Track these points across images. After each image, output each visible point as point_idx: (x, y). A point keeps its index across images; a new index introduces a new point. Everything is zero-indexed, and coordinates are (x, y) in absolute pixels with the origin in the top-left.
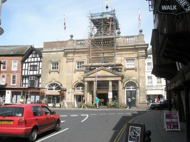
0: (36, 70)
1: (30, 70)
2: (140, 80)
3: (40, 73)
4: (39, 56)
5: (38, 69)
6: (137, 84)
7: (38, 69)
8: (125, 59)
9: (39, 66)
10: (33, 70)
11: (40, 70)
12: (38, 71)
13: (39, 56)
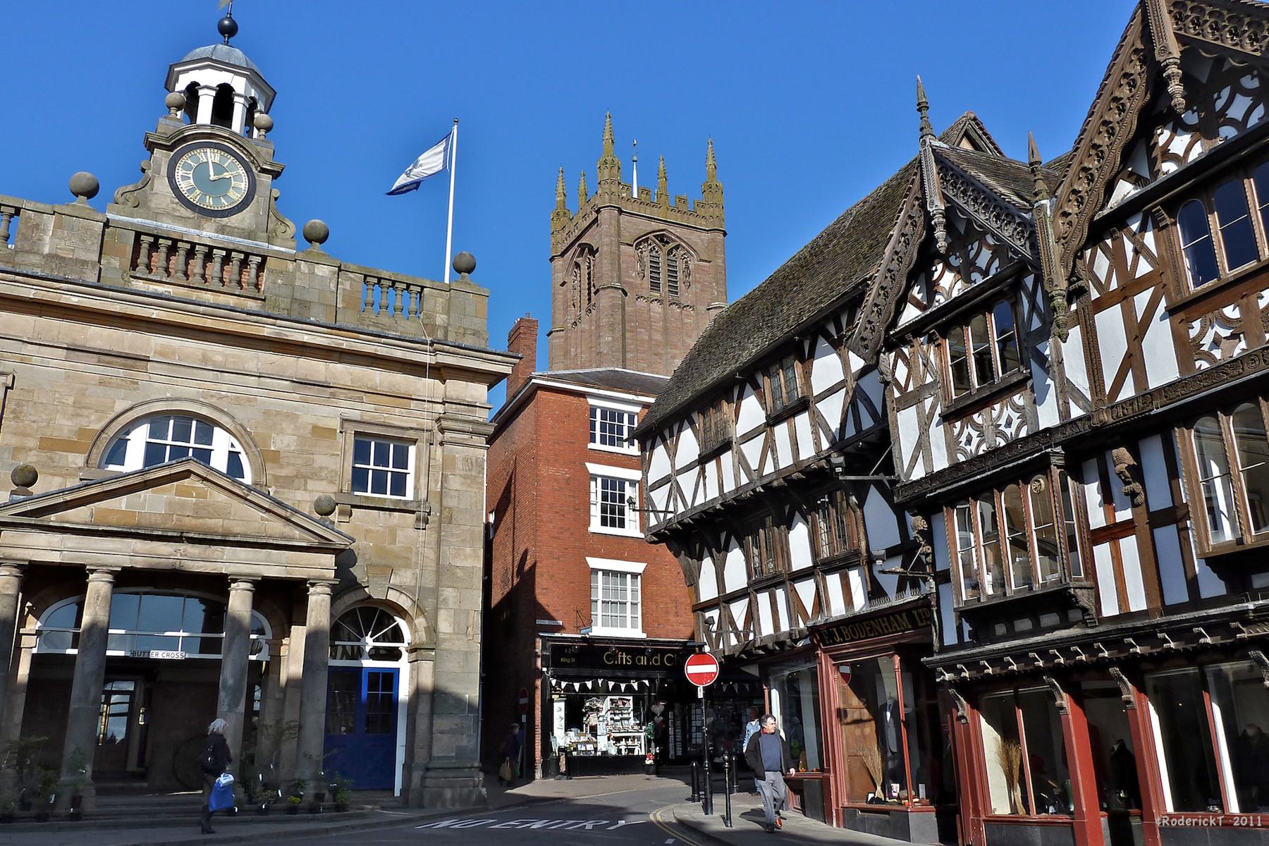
2: (448, 593)
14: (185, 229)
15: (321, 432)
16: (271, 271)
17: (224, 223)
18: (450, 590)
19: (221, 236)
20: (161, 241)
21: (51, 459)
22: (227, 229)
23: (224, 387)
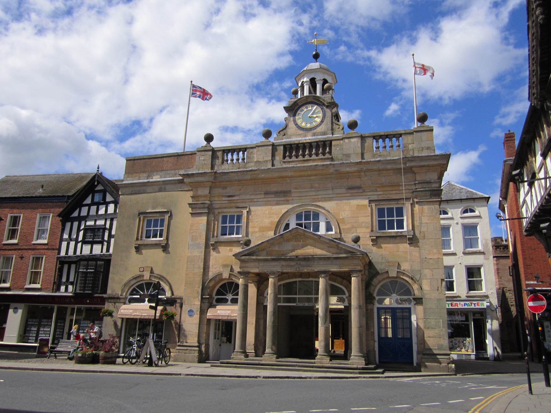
0: (102, 243)
1: (84, 242)
2: (427, 272)
3: (111, 251)
4: (112, 199)
5: (106, 238)
6: (415, 287)
7: (106, 238)
10: (92, 243)
11: (112, 240)
12: (105, 243)
13: (112, 199)
14: (300, 139)
16: (334, 145)
17: (315, 132)
18: (427, 270)
19: (314, 137)
20: (293, 146)
21: (263, 234)
22: (316, 134)
23: (320, 197)
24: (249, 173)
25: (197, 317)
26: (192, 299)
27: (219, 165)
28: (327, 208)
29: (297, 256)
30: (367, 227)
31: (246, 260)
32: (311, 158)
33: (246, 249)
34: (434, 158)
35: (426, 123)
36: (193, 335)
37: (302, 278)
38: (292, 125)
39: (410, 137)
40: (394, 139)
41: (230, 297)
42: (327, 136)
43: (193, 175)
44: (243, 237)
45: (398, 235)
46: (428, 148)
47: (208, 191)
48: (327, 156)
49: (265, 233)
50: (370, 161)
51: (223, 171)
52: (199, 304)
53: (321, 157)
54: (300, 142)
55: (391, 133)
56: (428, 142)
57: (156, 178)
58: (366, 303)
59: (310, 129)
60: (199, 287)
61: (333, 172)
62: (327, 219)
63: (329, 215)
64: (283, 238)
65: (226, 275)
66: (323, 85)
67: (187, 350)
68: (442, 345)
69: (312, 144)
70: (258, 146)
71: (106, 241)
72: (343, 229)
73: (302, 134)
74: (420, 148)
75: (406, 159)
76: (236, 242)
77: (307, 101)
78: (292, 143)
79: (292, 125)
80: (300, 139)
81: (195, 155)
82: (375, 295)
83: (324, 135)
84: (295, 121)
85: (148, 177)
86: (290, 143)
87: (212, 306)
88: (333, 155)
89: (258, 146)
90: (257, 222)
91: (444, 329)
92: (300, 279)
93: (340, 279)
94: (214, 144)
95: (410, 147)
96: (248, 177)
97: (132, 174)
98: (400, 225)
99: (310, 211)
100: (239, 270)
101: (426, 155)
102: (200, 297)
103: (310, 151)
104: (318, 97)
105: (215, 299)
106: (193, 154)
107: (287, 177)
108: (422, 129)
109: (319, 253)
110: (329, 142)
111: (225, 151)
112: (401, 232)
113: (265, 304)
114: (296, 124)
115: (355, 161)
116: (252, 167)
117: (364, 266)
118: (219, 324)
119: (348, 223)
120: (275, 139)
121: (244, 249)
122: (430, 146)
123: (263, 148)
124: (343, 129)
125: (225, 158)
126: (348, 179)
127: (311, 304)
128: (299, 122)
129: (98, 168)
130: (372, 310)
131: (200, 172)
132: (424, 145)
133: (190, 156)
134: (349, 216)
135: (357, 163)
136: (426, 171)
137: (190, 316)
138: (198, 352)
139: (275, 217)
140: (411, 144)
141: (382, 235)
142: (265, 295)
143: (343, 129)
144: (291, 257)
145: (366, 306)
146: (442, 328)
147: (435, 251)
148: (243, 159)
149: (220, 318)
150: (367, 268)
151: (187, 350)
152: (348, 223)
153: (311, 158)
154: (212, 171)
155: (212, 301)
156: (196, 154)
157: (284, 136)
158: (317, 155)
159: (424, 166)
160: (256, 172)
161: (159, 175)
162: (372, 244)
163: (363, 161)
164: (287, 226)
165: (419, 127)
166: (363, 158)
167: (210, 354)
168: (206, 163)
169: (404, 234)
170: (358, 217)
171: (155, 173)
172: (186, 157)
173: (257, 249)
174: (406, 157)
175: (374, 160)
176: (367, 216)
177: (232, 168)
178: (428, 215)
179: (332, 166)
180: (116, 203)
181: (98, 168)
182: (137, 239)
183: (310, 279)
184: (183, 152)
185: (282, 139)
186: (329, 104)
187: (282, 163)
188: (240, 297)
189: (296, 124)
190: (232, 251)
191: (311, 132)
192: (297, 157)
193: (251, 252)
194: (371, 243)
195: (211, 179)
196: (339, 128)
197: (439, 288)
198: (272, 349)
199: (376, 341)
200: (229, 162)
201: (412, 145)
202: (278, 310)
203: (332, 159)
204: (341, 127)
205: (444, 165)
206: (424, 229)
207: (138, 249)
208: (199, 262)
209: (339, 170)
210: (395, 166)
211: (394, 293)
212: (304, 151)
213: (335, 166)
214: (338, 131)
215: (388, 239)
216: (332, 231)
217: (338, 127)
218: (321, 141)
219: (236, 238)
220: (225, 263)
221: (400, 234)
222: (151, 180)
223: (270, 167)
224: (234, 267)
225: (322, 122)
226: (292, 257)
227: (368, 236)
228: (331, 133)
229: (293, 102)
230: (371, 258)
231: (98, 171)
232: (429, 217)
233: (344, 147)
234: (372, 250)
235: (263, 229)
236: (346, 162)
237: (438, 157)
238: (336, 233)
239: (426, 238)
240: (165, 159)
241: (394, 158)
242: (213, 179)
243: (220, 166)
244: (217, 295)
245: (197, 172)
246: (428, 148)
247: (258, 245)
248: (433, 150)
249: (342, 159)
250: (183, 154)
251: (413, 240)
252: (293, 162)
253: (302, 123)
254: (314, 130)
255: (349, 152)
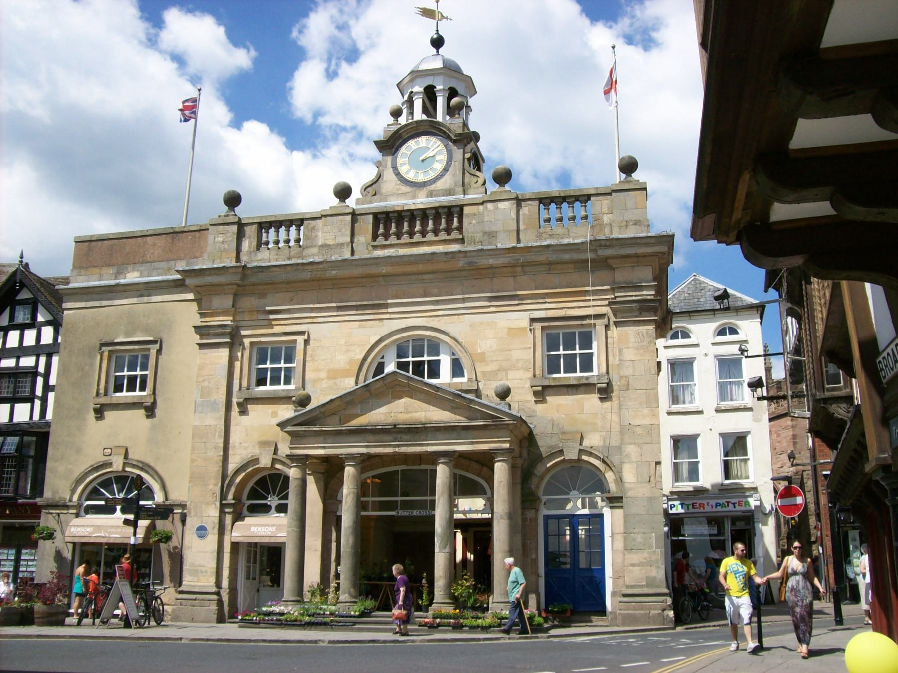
0: (31, 400)
3: (49, 416)
5: (39, 392)
6: (610, 476)
7: (39, 392)
8: (538, 326)
9: (47, 376)
11: (51, 396)
12: (38, 403)
14: (405, 202)
15: (513, 332)
16: (468, 215)
17: (432, 189)
18: (632, 446)
19: (430, 199)
21: (335, 384)
22: (434, 193)
24: (308, 267)
25: (212, 539)
26: (203, 506)
27: (251, 252)
28: (452, 334)
29: (395, 425)
30: (527, 370)
31: (301, 432)
32: (424, 239)
33: (300, 412)
34: (644, 241)
35: (635, 176)
36: (206, 572)
37: (407, 465)
38: (389, 175)
39: (605, 202)
40: (577, 204)
41: (273, 501)
42: (455, 197)
43: (201, 270)
44: (297, 389)
45: (581, 383)
46: (637, 223)
47: (231, 303)
48: (455, 235)
49: (338, 381)
50: (532, 247)
51: (260, 264)
52: (217, 515)
53: (442, 238)
54: (405, 209)
55: (572, 194)
56: (636, 211)
57: (132, 277)
58: (524, 509)
59: (424, 185)
60: (216, 485)
61: (464, 267)
62: (454, 354)
63: (456, 346)
64: (370, 392)
65: (265, 461)
66: (449, 99)
67: (195, 599)
68: (654, 578)
69: (427, 212)
70: (326, 216)
71: (38, 398)
72: (483, 373)
73: (408, 193)
74: (622, 221)
75: (596, 244)
76: (285, 399)
77: (416, 130)
78: (389, 210)
79: (389, 175)
80: (405, 202)
81: (206, 232)
82: (540, 493)
83: (450, 195)
84: (395, 168)
85: (117, 275)
86: (385, 210)
87: (238, 517)
88: (465, 234)
89: (326, 216)
90: (323, 360)
91: (659, 550)
92: (404, 467)
93: (476, 466)
94: (242, 211)
95: (606, 219)
96: (307, 275)
97: (87, 268)
98: (587, 364)
99: (423, 340)
100: (288, 452)
101: (632, 236)
102: (218, 504)
103: (424, 224)
104: (438, 123)
105: (247, 505)
106: (202, 230)
107: (379, 276)
108: (627, 187)
109: (436, 419)
110: (458, 209)
111: (263, 226)
112: (587, 378)
113: (338, 514)
114: (398, 175)
115: (504, 246)
116: (313, 255)
117: (521, 441)
118: (256, 552)
119: (492, 361)
120: (358, 201)
121: (297, 413)
122: (640, 219)
123: (335, 218)
124: (484, 184)
125: (264, 239)
126: (492, 278)
127: (423, 513)
128: (403, 170)
129: (22, 257)
130: (536, 520)
131: (215, 266)
132: (630, 216)
133: (197, 234)
134: (494, 349)
135: (509, 249)
136: (633, 265)
137: (201, 537)
138: (217, 603)
139: (358, 351)
140: (607, 214)
141: (552, 384)
142: (339, 497)
143: (484, 184)
144: (384, 427)
145: (523, 514)
146: (654, 549)
147: (646, 411)
148: (298, 241)
149: (256, 540)
150: (526, 444)
151: (195, 599)
152: (492, 361)
153: (424, 239)
154: (239, 264)
155: (242, 509)
156: (207, 229)
157: (375, 197)
158: (436, 232)
159: (628, 256)
160: (321, 266)
161: (138, 271)
162: (535, 401)
163: (519, 246)
164: (380, 368)
165: (623, 182)
166: (519, 241)
167: (239, 606)
168: (227, 247)
169: (591, 381)
170: (510, 350)
171: (130, 268)
172: (189, 236)
173: (321, 412)
174: (595, 240)
175: (538, 244)
176: (526, 348)
177: (277, 257)
178: (635, 345)
179: (461, 255)
180: (56, 324)
181: (22, 257)
182: (98, 394)
183: (423, 467)
184: (184, 227)
185: (371, 203)
186: (458, 138)
187: (370, 248)
188: (292, 502)
189: (398, 175)
190: (277, 416)
191: (425, 189)
192: (398, 236)
193: (310, 418)
194: (534, 399)
195: (237, 279)
196: (477, 183)
197: (652, 479)
198: (350, 593)
199: (541, 577)
200: (271, 245)
201: (608, 215)
202: (362, 526)
203: (462, 241)
204: (481, 182)
205: (664, 254)
206: (627, 372)
207: (100, 412)
208: (215, 436)
209: (476, 263)
210: (576, 256)
211: (574, 489)
212: (412, 226)
213: (468, 254)
214: (475, 188)
215: (564, 390)
216: (463, 376)
217: (475, 179)
218: (444, 207)
219: (283, 390)
220: (264, 438)
221: (585, 382)
222: (122, 281)
223: (346, 257)
224: (279, 446)
225: (446, 170)
226: (387, 427)
227: (528, 385)
228: (462, 192)
229: (393, 132)
230: (532, 426)
231: (21, 262)
232: (637, 350)
233: (486, 219)
234: (534, 411)
235: (334, 374)
236: (489, 247)
237: (652, 241)
238: (470, 380)
239: (630, 387)
240: (149, 238)
241: (576, 241)
242: (241, 280)
243: (253, 254)
244: (249, 498)
245: (210, 266)
246: (637, 223)
247: (324, 405)
248: (645, 226)
249: (481, 242)
250: (182, 230)
251: (605, 393)
252: (391, 246)
253: (407, 172)
254: (431, 185)
255: (494, 229)
